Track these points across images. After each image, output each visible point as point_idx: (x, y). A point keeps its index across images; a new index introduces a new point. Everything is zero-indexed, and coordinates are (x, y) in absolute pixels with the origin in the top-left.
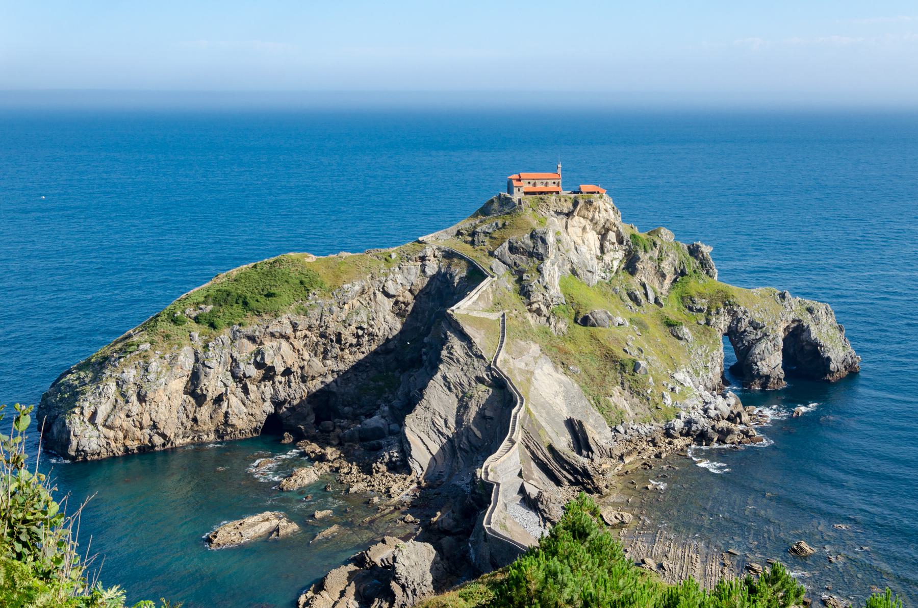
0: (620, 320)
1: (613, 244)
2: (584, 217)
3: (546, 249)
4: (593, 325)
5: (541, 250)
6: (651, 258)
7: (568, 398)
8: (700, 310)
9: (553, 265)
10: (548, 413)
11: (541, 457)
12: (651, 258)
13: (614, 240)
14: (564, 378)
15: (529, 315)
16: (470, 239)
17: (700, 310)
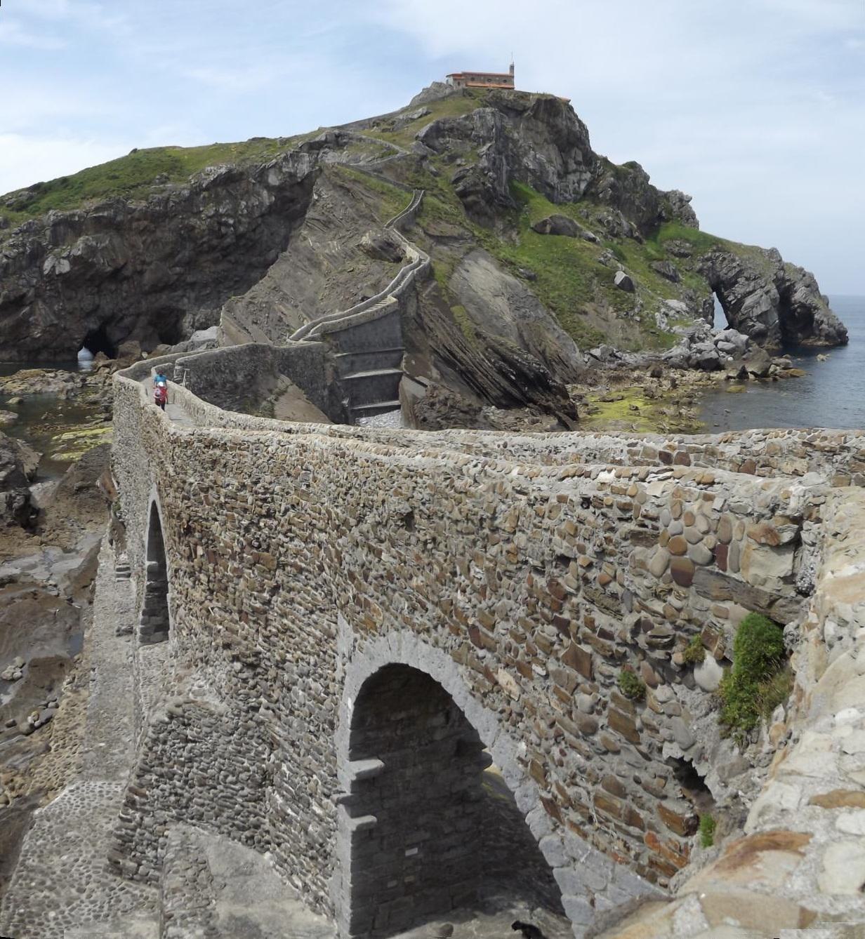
2: (542, 121)
5: (482, 133)
7: (514, 300)
9: (500, 153)
13: (580, 158)
14: (510, 279)
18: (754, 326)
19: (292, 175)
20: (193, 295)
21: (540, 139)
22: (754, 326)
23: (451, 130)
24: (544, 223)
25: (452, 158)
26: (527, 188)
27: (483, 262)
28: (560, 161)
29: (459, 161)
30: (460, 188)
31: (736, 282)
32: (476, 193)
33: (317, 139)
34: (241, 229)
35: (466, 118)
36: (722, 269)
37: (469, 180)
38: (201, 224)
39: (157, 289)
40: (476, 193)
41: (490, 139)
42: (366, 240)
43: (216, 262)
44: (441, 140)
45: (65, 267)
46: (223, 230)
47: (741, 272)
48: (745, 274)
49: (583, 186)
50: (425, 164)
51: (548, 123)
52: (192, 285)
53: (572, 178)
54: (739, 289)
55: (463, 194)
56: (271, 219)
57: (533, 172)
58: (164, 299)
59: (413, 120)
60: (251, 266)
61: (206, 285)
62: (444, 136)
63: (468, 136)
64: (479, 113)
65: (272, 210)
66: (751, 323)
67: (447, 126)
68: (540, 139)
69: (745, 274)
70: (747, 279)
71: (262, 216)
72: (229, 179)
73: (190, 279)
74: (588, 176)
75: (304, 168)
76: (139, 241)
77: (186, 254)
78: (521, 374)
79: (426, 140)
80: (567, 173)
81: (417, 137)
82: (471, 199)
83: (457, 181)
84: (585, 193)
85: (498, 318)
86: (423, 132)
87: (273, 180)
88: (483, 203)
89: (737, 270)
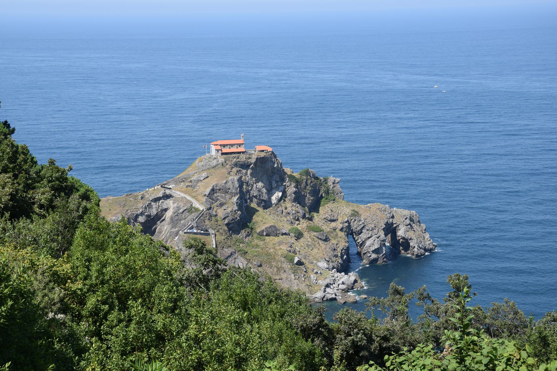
0: (284, 231)
1: (278, 182)
4: (267, 235)
5: (234, 191)
13: (278, 179)
18: (370, 256)
19: (149, 216)
22: (370, 256)
24: (263, 231)
26: (254, 205)
31: (362, 232)
33: (158, 196)
35: (226, 183)
36: (354, 225)
37: (230, 218)
41: (237, 194)
47: (363, 227)
48: (367, 228)
54: (363, 236)
57: (256, 197)
59: (201, 180)
62: (216, 193)
63: (227, 192)
64: (231, 180)
66: (369, 255)
67: (218, 188)
69: (367, 228)
70: (368, 230)
75: (154, 212)
82: (231, 226)
83: (224, 219)
89: (362, 226)
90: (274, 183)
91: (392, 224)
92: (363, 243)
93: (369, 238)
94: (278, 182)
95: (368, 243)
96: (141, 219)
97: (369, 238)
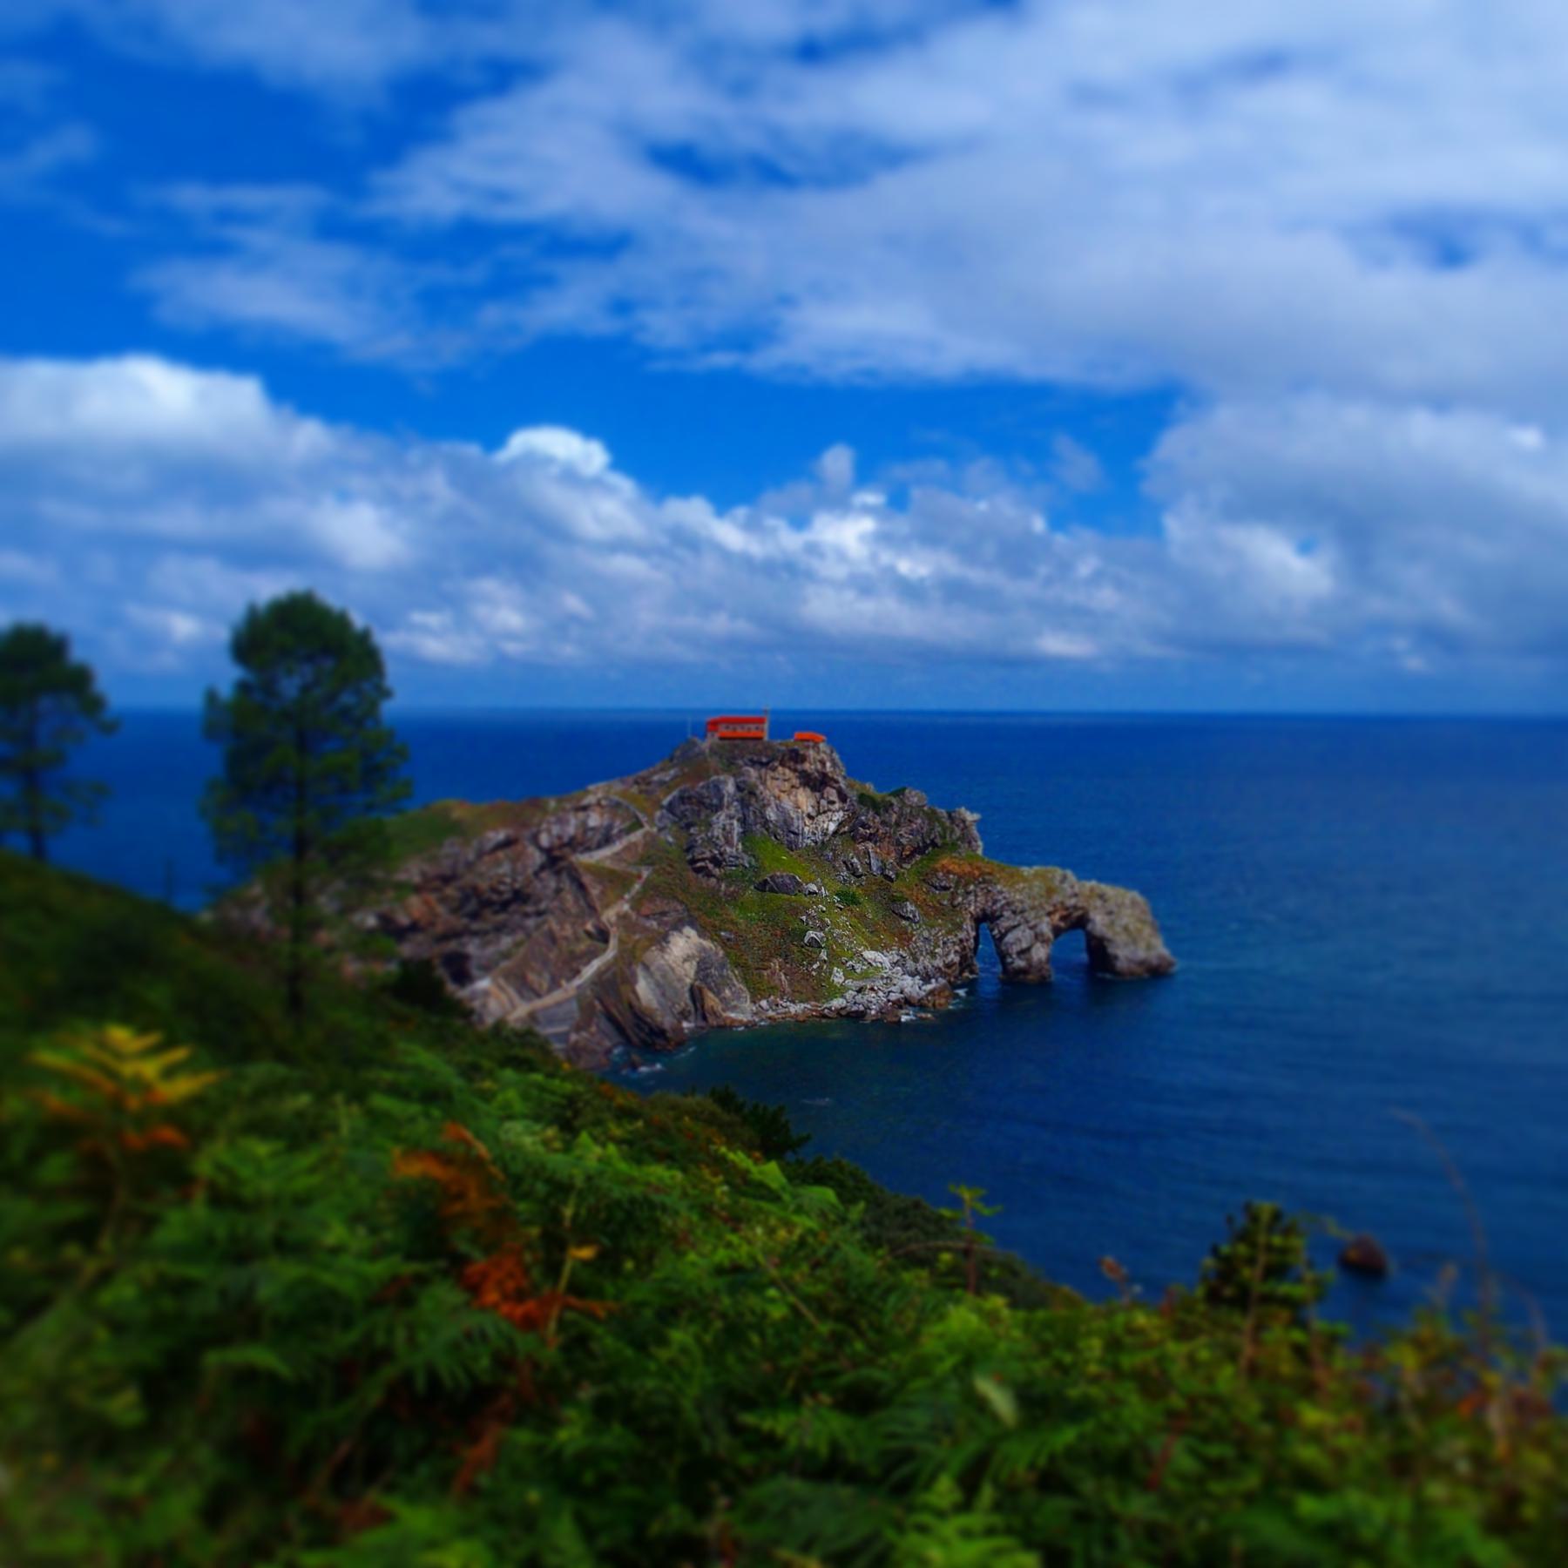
0: (814, 888)
1: (833, 803)
3: (721, 799)
4: (772, 890)
5: (715, 801)
6: (883, 823)
8: (945, 888)
9: (731, 818)
10: (664, 976)
11: (614, 1011)
12: (883, 823)
13: (834, 797)
14: (707, 944)
15: (692, 874)
16: (644, 787)
17: (945, 888)
19: (559, 837)
20: (477, 941)
21: (787, 785)
23: (690, 798)
25: (689, 826)
27: (688, 931)
28: (813, 802)
29: (692, 830)
30: (689, 857)
32: (703, 860)
34: (517, 886)
38: (484, 885)
39: (445, 937)
40: (703, 860)
42: (589, 927)
43: (496, 912)
44: (683, 808)
45: (371, 921)
46: (502, 888)
49: (832, 827)
50: (662, 836)
51: (795, 770)
52: (475, 934)
53: (821, 818)
55: (693, 861)
56: (544, 875)
58: (452, 945)
60: (527, 915)
61: (486, 933)
65: (543, 868)
68: (787, 785)
71: (536, 874)
72: (508, 843)
73: (475, 926)
74: (839, 816)
76: (432, 897)
77: (472, 905)
78: (651, 1029)
79: (670, 808)
80: (819, 813)
81: (662, 807)
84: (835, 833)
85: (680, 980)
86: (665, 802)
87: (544, 840)
88: (711, 866)
90: (823, 802)
91: (1075, 908)
92: (1003, 936)
93: (1014, 927)
94: (833, 803)
95: (1010, 938)
96: (544, 840)
97: (1014, 927)
